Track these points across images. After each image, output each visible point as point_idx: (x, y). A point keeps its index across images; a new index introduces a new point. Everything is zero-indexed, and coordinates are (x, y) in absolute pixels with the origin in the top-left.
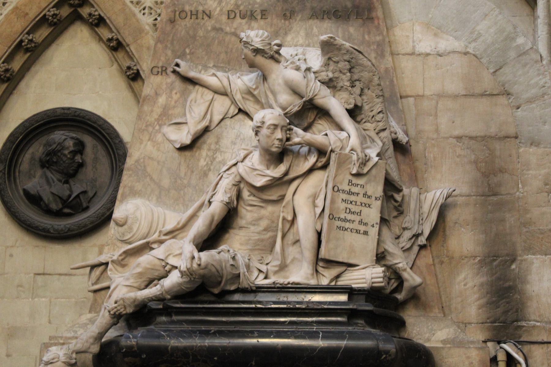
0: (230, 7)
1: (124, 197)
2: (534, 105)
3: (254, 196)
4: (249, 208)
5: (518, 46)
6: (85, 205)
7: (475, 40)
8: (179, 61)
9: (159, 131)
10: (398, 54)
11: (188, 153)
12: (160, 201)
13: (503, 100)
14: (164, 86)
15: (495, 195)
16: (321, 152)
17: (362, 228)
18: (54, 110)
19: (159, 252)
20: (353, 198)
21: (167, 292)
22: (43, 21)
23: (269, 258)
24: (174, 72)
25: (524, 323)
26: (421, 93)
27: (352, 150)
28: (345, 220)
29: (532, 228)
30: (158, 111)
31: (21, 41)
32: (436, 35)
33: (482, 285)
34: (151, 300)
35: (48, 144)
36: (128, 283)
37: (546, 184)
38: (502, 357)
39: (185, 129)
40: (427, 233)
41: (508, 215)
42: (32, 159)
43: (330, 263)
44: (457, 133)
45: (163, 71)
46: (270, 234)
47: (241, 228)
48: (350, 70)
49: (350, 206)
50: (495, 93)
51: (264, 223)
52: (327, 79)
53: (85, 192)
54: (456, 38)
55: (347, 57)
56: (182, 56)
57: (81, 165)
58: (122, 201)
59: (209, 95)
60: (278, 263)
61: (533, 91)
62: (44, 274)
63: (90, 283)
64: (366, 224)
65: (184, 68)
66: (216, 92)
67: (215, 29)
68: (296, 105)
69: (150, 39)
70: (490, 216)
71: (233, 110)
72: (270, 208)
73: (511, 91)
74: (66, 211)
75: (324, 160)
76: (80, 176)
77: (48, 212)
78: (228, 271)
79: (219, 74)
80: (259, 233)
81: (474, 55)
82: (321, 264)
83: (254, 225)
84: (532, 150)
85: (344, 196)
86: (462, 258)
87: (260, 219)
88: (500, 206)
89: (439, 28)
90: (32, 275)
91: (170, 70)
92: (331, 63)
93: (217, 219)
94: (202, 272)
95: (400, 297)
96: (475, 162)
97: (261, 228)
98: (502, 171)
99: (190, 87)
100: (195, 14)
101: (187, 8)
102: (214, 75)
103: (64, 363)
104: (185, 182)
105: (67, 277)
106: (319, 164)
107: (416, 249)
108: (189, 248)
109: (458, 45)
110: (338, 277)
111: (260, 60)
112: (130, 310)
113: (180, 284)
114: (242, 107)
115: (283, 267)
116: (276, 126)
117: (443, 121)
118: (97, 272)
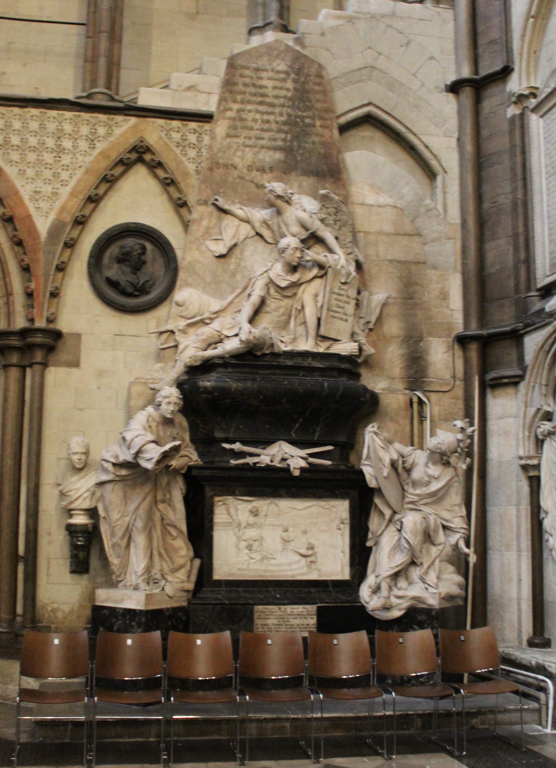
0: (249, 163)
1: (181, 287)
2: (435, 244)
3: (278, 293)
4: (273, 300)
5: (426, 205)
6: (148, 290)
7: (401, 199)
8: (217, 197)
9: (203, 244)
10: (353, 204)
11: (222, 260)
12: (204, 290)
13: (417, 239)
14: (206, 214)
15: (411, 298)
16: (321, 267)
17: (344, 317)
18: (128, 224)
19: (216, 325)
20: (340, 298)
21: (228, 353)
22: (121, 162)
23: (284, 333)
24: (214, 204)
25: (426, 379)
26: (367, 229)
27: (342, 267)
28: (335, 312)
29: (433, 321)
30: (202, 230)
31: (106, 175)
32: (377, 193)
33: (403, 355)
34: (213, 358)
35: (122, 247)
36: (195, 346)
37: (441, 294)
38: (415, 399)
39: (221, 244)
40: (373, 320)
41: (418, 312)
42: (111, 256)
43: (325, 338)
44: (389, 257)
45: (206, 203)
46: (285, 317)
47: (267, 312)
48: (335, 214)
49: (339, 303)
50: (412, 234)
51: (282, 311)
52: (321, 218)
53: (147, 281)
54: (390, 197)
55: (335, 206)
56: (218, 193)
57: (144, 262)
58: (179, 289)
59: (237, 222)
60: (292, 337)
61: (435, 235)
62: (120, 335)
63: (159, 343)
64: (346, 315)
65: (221, 203)
66: (241, 220)
67: (239, 177)
68: (305, 235)
69: (194, 181)
70: (408, 312)
71: (252, 233)
72: (286, 302)
73: (422, 234)
74: (136, 293)
75: (322, 272)
76: (144, 270)
77: (124, 293)
78: (268, 342)
79: (244, 208)
80: (279, 316)
81: (401, 209)
82: (319, 339)
83: (275, 311)
84: (433, 272)
85: (335, 296)
86: (392, 337)
87: (279, 308)
88: (415, 306)
89: (379, 189)
90: (112, 335)
91: (210, 202)
92: (324, 208)
93: (257, 306)
94: (255, 341)
95: (360, 360)
96: (400, 277)
97: (280, 314)
98: (416, 284)
99: (223, 215)
100: (226, 166)
101: (221, 161)
102: (241, 209)
103: (177, 397)
104: (221, 279)
105: (136, 338)
106: (320, 275)
107: (367, 330)
108: (246, 326)
109: (390, 201)
110: (328, 348)
111: (279, 202)
112: (198, 363)
113: (238, 349)
114: (259, 231)
115: (294, 340)
116: (296, 248)
117: (381, 249)
118: (165, 336)
